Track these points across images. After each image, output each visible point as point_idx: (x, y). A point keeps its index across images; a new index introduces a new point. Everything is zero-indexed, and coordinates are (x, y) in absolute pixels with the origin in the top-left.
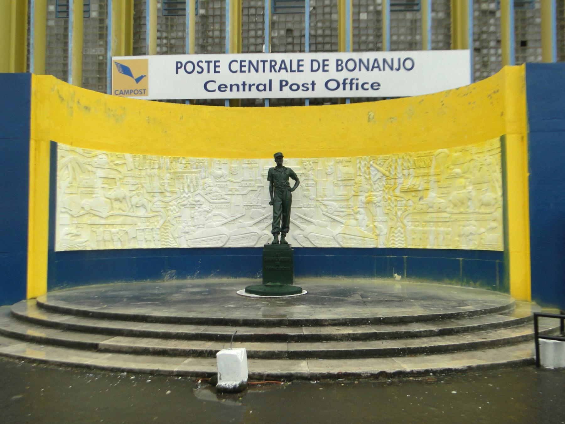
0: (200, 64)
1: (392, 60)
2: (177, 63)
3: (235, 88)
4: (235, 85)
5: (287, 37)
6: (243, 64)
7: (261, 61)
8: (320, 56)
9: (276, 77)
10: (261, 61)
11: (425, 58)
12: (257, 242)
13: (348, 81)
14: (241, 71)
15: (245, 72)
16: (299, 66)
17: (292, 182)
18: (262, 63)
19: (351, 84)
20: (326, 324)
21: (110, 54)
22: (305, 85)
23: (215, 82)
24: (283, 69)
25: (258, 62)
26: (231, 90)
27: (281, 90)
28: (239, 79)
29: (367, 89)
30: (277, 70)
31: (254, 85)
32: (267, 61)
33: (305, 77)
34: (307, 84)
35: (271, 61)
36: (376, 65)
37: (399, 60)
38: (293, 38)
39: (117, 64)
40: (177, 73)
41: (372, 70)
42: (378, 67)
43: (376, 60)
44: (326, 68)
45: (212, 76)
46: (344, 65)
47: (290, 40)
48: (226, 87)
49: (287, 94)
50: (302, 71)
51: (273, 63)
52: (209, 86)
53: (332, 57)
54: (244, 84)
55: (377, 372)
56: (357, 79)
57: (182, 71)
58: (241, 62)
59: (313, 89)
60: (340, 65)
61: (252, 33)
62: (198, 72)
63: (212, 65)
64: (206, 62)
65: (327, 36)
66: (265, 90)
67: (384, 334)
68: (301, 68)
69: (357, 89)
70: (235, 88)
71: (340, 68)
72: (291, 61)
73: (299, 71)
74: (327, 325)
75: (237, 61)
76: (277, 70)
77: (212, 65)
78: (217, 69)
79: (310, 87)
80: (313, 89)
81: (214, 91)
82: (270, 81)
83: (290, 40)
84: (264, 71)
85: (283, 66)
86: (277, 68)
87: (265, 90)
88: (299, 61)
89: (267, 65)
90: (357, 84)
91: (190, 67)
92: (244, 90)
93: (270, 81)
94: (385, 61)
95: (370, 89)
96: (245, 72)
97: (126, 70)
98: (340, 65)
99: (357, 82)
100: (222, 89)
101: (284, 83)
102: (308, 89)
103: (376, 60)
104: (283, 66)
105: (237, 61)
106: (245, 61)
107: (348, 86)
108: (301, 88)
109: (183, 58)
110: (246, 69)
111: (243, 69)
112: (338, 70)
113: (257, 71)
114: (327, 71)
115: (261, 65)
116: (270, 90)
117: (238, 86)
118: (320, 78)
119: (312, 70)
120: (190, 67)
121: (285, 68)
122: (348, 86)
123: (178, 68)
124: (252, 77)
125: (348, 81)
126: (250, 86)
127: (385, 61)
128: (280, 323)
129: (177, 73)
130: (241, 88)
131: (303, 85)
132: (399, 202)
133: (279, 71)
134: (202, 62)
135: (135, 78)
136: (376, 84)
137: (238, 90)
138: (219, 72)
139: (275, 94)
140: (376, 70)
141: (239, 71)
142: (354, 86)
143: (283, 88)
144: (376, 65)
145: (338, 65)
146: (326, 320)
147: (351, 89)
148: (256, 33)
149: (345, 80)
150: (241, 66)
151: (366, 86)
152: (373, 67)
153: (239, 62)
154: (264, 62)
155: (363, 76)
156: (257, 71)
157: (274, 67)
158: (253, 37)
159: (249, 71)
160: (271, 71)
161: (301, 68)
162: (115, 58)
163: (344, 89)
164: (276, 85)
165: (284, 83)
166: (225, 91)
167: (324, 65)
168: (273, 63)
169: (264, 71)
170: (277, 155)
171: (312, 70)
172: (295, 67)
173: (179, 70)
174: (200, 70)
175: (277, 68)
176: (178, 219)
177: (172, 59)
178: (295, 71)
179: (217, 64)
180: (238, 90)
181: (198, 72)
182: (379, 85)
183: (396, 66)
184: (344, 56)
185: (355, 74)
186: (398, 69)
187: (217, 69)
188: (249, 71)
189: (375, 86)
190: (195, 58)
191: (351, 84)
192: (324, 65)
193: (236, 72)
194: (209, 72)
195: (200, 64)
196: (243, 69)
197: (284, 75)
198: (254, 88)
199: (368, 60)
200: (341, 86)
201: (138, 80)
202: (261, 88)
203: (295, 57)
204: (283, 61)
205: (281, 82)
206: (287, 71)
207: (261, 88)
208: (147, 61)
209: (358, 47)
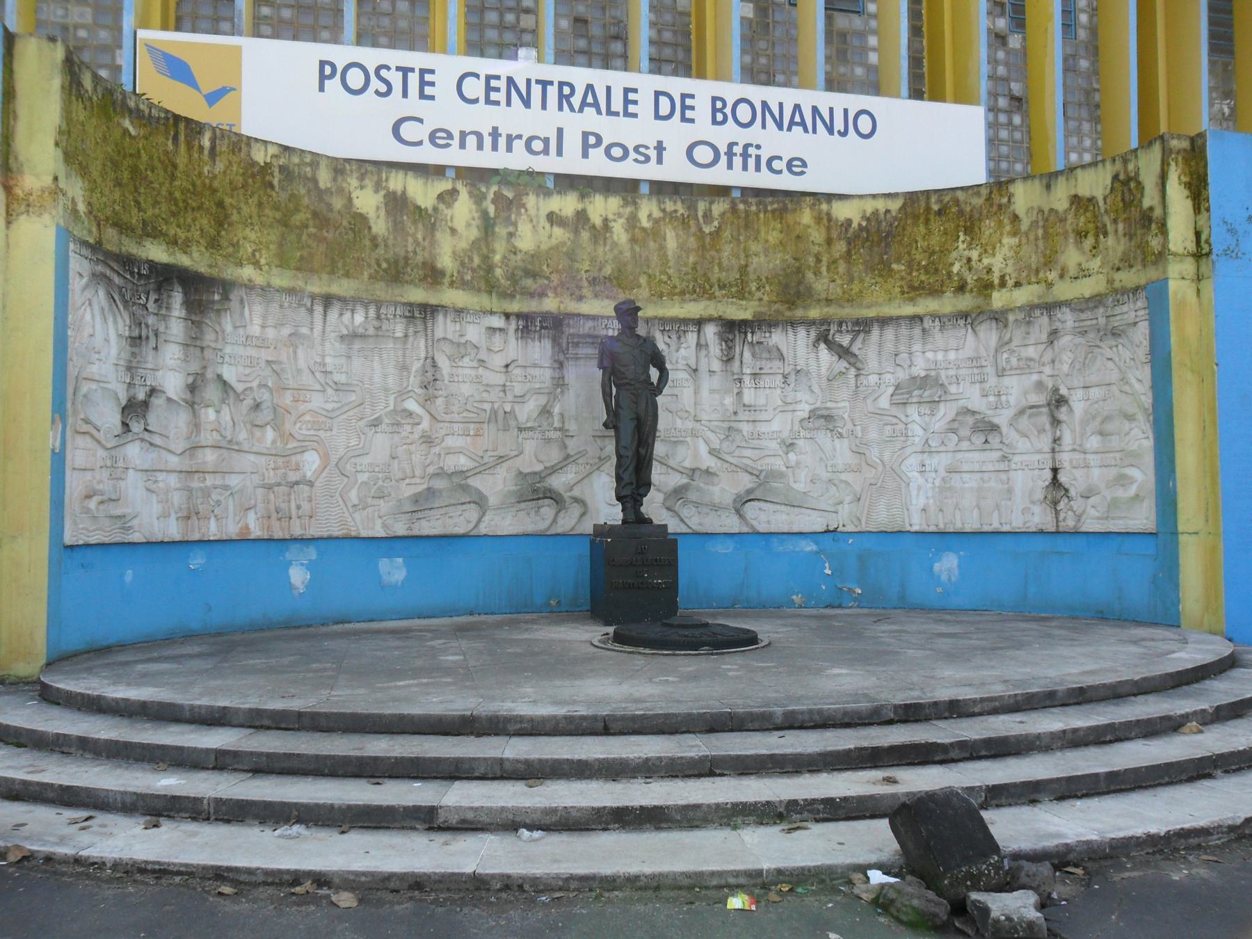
0: (383, 73)
1: (831, 110)
2: (322, 64)
3: (471, 141)
4: (471, 133)
5: (578, 36)
6: (494, 83)
7: (538, 82)
8: (677, 85)
9: (576, 123)
10: (538, 82)
11: (897, 113)
12: (555, 521)
13: (738, 150)
14: (488, 101)
15: (497, 103)
16: (627, 102)
17: (654, 374)
18: (540, 87)
19: (745, 155)
20: (977, 710)
21: (128, 21)
22: (642, 150)
23: (421, 121)
24: (590, 105)
25: (529, 81)
26: (462, 145)
27: (585, 155)
28: (483, 118)
29: (780, 172)
30: (577, 107)
31: (519, 137)
32: (551, 83)
33: (640, 129)
34: (647, 148)
35: (561, 84)
36: (797, 119)
37: (846, 111)
38: (590, 40)
39: (150, 48)
40: (322, 89)
41: (789, 129)
42: (803, 123)
43: (797, 107)
44: (689, 114)
45: (412, 105)
46: (728, 110)
47: (582, 43)
48: (450, 136)
49: (597, 165)
50: (635, 115)
51: (566, 90)
52: (407, 131)
53: (703, 90)
54: (495, 133)
55: (1239, 822)
56: (758, 147)
57: (334, 85)
58: (489, 78)
59: (660, 161)
60: (721, 110)
61: (492, 17)
62: (377, 92)
63: (414, 79)
64: (398, 69)
65: (665, 44)
66: (546, 151)
67: (1128, 725)
68: (631, 109)
69: (758, 169)
70: (471, 141)
71: (720, 117)
72: (609, 89)
73: (627, 114)
74: (980, 714)
75: (477, 76)
76: (577, 107)
77: (414, 79)
78: (428, 90)
79: (653, 154)
80: (660, 161)
81: (420, 143)
82: (560, 131)
83: (582, 43)
84: (544, 107)
85: (590, 99)
86: (576, 101)
87: (546, 151)
88: (627, 91)
89: (552, 91)
90: (758, 158)
91: (356, 79)
92: (495, 147)
93: (560, 131)
94: (815, 110)
95: (785, 171)
96: (497, 103)
97: (177, 69)
98: (721, 110)
99: (758, 152)
100: (438, 141)
101: (592, 140)
102: (648, 159)
103: (797, 107)
104: (590, 99)
105: (477, 76)
106: (498, 78)
107: (738, 161)
108: (633, 155)
109: (341, 54)
110: (500, 96)
111: (494, 96)
112: (714, 122)
113: (527, 103)
114: (692, 121)
115: (536, 90)
116: (560, 153)
117: (479, 136)
118: (676, 135)
119: (657, 116)
120: (356, 79)
121: (596, 105)
122: (738, 161)
123: (323, 78)
124: (514, 118)
125: (738, 150)
126: (510, 139)
127: (815, 110)
128: (911, 714)
129: (322, 89)
130: (488, 141)
131: (636, 149)
132: (889, 427)
133: (581, 110)
134: (388, 68)
135: (205, 92)
136: (799, 163)
137: (480, 146)
138: (432, 98)
139: (571, 163)
140: (797, 130)
141: (482, 99)
142: (751, 162)
143: (591, 151)
144: (797, 120)
145: (715, 110)
146: (974, 701)
147: (745, 168)
148: (501, 15)
149: (731, 145)
150: (489, 89)
151: (776, 165)
152: (792, 123)
153: (483, 78)
154: (545, 84)
155: (772, 141)
156: (527, 103)
157: (568, 97)
158: (493, 27)
159: (509, 103)
160: (561, 108)
161: (631, 109)
162: (142, 34)
163: (730, 166)
164: (573, 142)
165: (592, 140)
166: (448, 145)
167: (684, 106)
168: (566, 90)
169: (544, 107)
170: (624, 307)
171: (657, 116)
172: (617, 105)
173: (326, 82)
174: (383, 88)
175: (576, 101)
176: (358, 460)
177: (308, 54)
178: (617, 114)
179: (428, 77)
180: (480, 146)
181: (377, 92)
182: (804, 164)
183: (839, 125)
184: (731, 91)
185: (754, 134)
186: (844, 134)
187: (428, 90)
188: (509, 103)
189: (796, 165)
190: (371, 56)
191: (745, 155)
192: (684, 107)
193: (476, 101)
194: (405, 95)
195: (383, 73)
196: (494, 96)
197: (591, 120)
198: (519, 145)
199: (781, 105)
200: (724, 159)
201: (213, 98)
202: (537, 145)
203: (617, 79)
204: (590, 88)
205: (585, 135)
206: (599, 112)
207: (537, 145)
208: (238, 50)
209: (753, 75)
